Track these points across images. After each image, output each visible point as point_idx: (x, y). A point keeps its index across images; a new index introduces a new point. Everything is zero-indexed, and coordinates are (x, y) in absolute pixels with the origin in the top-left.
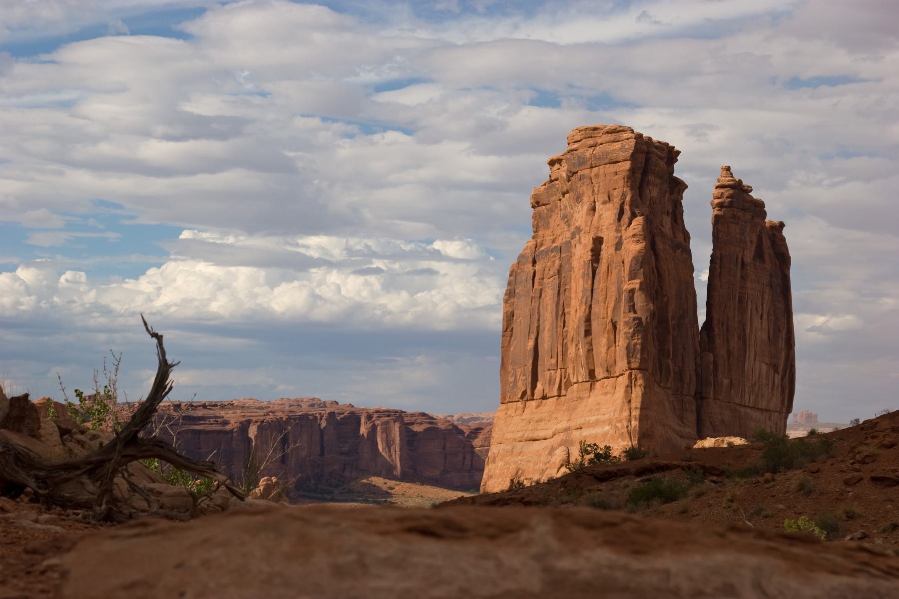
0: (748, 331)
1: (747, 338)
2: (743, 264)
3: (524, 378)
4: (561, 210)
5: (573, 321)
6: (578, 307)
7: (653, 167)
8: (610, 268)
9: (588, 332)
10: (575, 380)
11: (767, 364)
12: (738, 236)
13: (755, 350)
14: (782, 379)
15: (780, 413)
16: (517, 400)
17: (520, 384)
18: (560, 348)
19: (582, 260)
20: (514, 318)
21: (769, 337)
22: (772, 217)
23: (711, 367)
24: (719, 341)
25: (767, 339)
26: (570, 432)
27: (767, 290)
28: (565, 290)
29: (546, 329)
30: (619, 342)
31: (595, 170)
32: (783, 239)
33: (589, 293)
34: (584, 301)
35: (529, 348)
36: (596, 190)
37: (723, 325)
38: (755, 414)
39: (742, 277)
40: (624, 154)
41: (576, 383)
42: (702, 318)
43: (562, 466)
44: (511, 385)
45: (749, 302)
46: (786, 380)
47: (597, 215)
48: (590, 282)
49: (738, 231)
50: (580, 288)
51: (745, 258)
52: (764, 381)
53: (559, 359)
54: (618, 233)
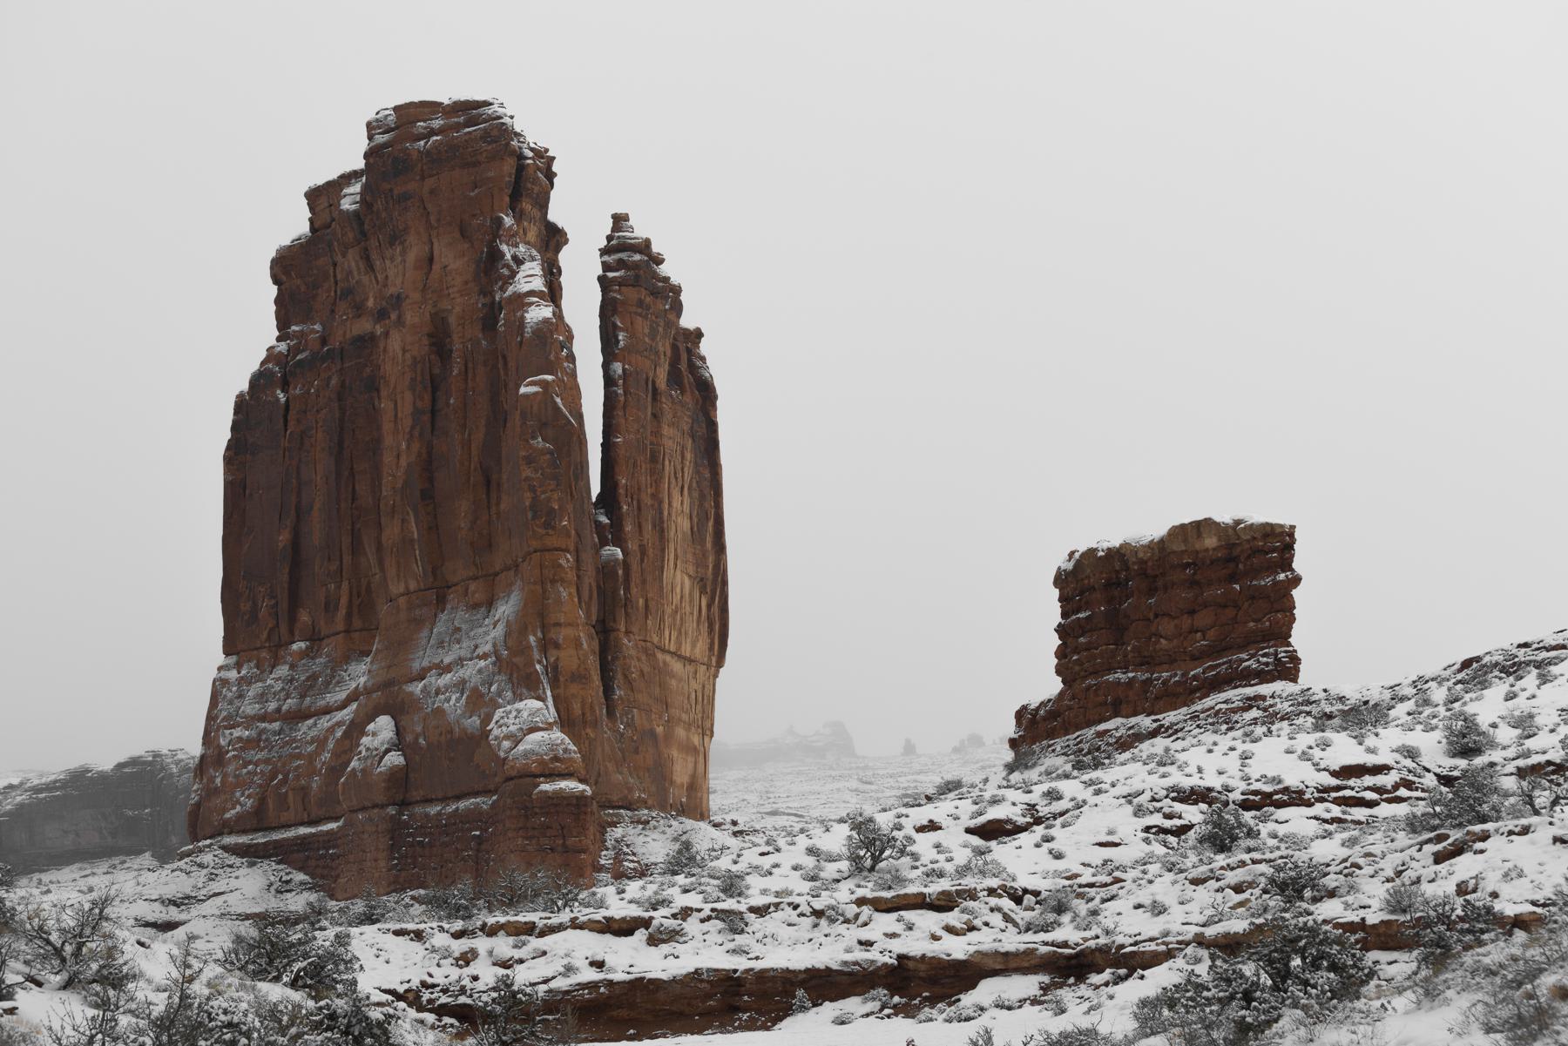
0: (666, 513)
1: (665, 525)
2: (655, 391)
3: (273, 602)
4: (336, 283)
5: (394, 476)
6: (404, 446)
7: (529, 185)
8: (470, 365)
9: (427, 495)
10: (402, 590)
11: (690, 576)
12: (647, 339)
13: (676, 550)
14: (709, 606)
15: (709, 666)
16: (259, 645)
17: (263, 612)
18: (346, 541)
19: (408, 355)
20: (247, 492)
21: (692, 529)
22: (687, 321)
23: (620, 572)
24: (628, 528)
25: (689, 532)
26: (396, 688)
27: (689, 443)
28: (353, 430)
29: (317, 506)
30: (498, 504)
31: (430, 183)
32: (703, 359)
33: (426, 418)
34: (416, 433)
35: (281, 545)
36: (432, 218)
37: (632, 498)
38: (677, 666)
39: (654, 415)
40: (490, 147)
41: (403, 595)
42: (595, 488)
43: (387, 751)
44: (246, 617)
45: (667, 462)
46: (715, 609)
47: (436, 267)
48: (427, 397)
49: (647, 331)
50: (406, 409)
51: (658, 382)
52: (688, 608)
53: (344, 561)
54: (485, 296)
